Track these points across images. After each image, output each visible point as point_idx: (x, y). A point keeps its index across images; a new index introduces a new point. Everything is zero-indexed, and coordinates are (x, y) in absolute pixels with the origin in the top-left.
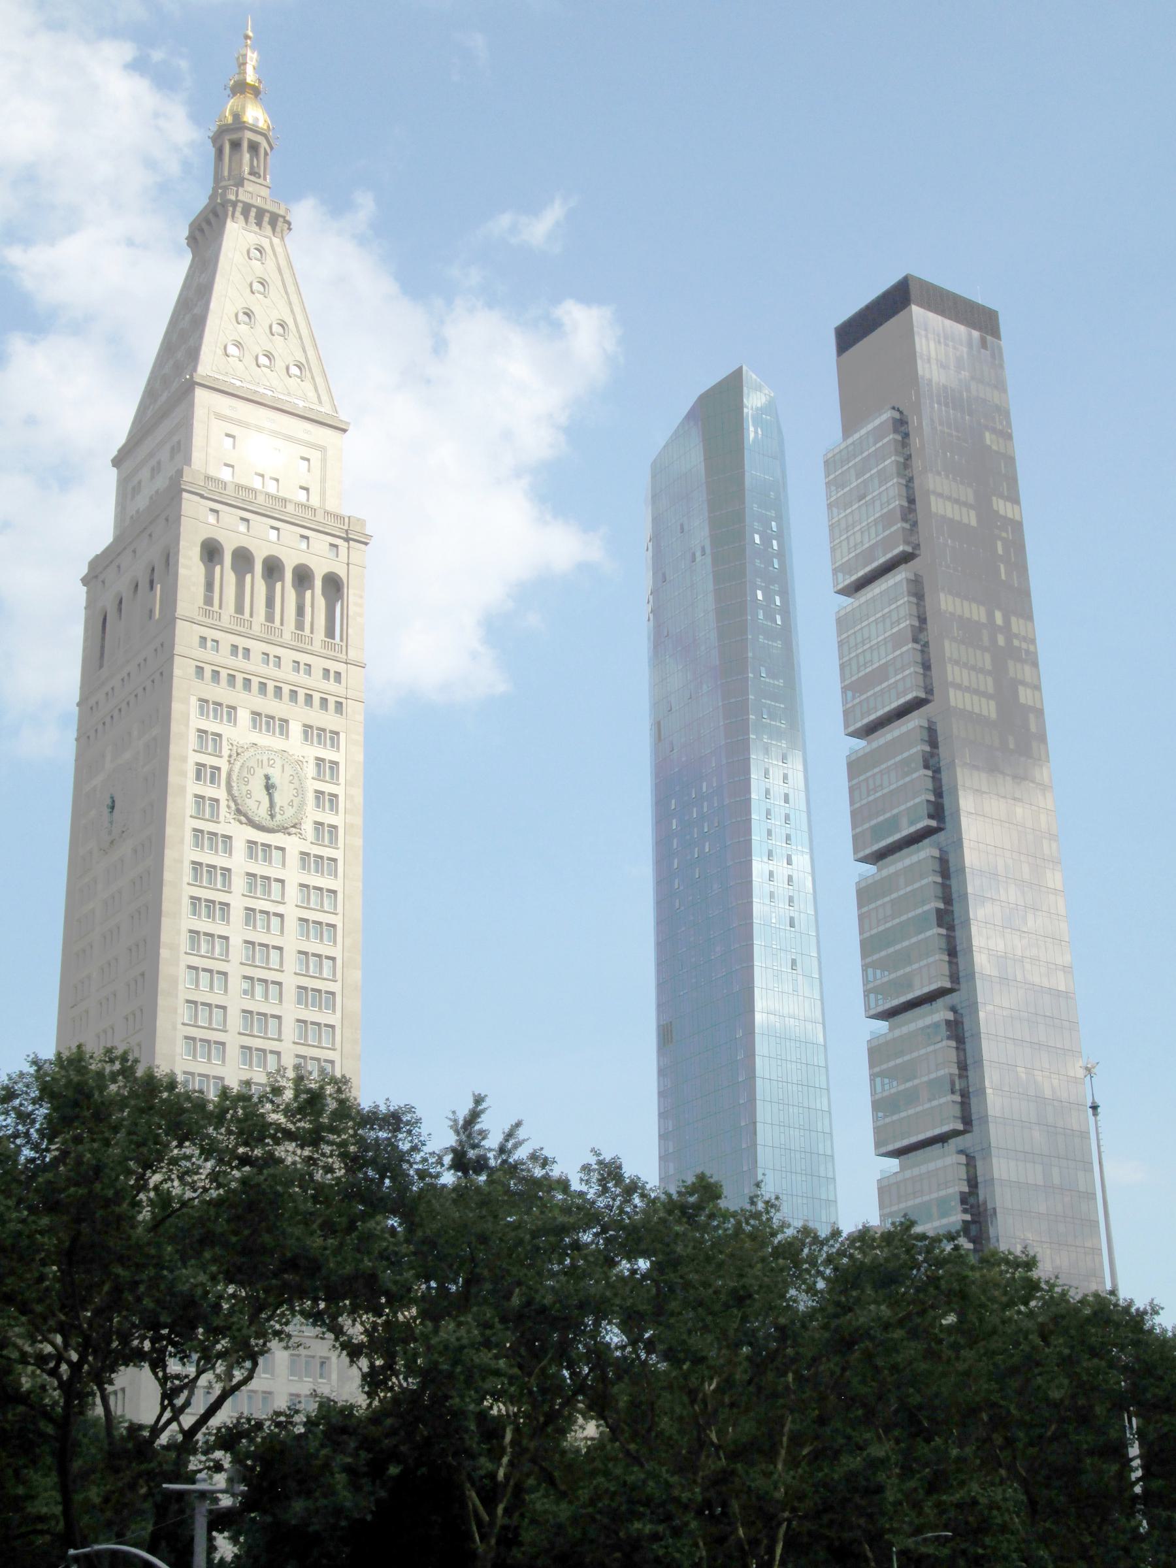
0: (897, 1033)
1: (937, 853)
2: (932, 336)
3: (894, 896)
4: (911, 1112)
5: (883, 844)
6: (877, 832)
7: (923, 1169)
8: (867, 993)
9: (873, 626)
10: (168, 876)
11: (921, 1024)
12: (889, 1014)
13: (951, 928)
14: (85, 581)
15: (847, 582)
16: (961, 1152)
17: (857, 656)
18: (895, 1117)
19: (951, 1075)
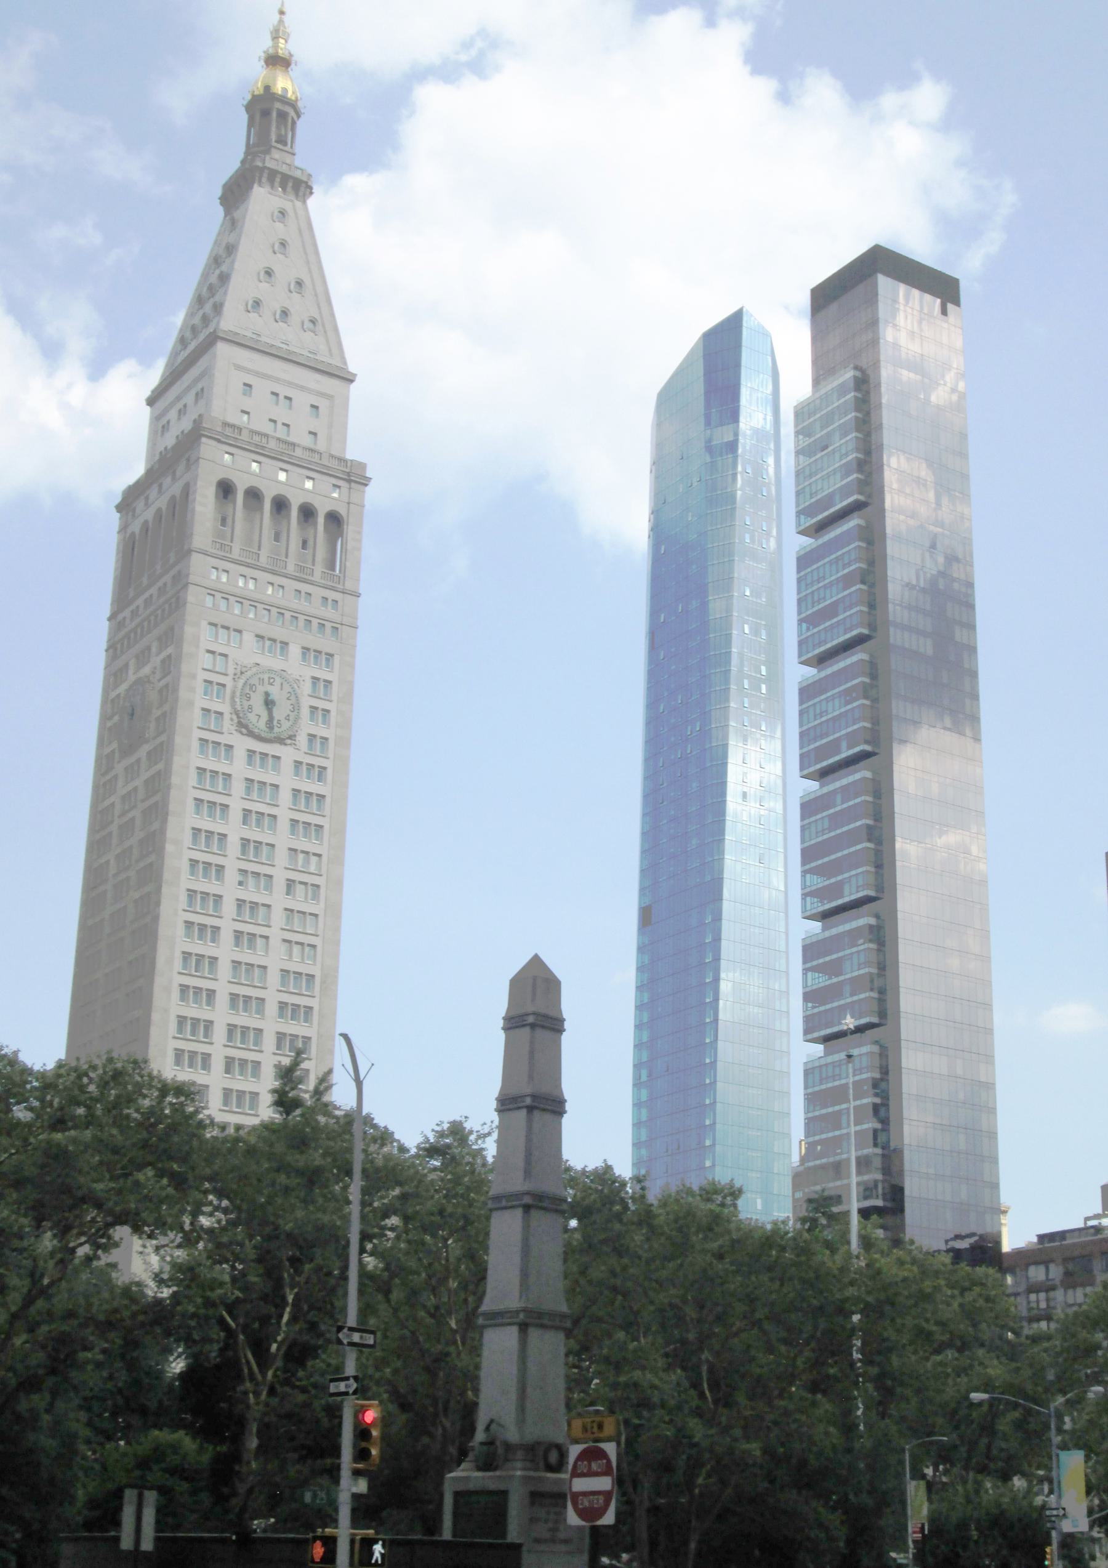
0: (827, 934)
3: (832, 811)
4: (836, 1004)
5: (825, 764)
6: (821, 753)
9: (827, 566)
10: (175, 780)
11: (847, 927)
13: (879, 842)
15: (808, 524)
16: (876, 1042)
17: (813, 592)
18: (822, 1008)
19: (871, 974)
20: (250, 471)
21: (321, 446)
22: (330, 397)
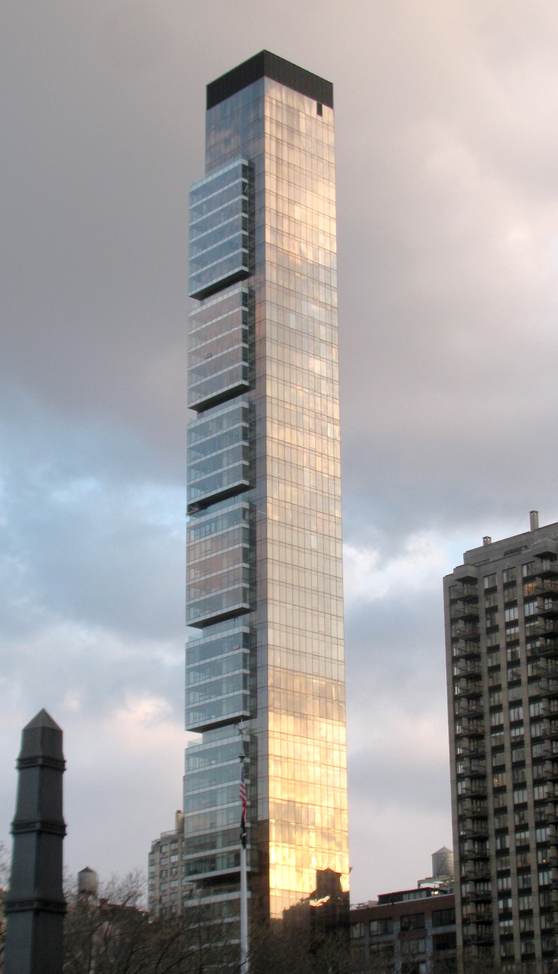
0: (208, 640)
1: (246, 506)
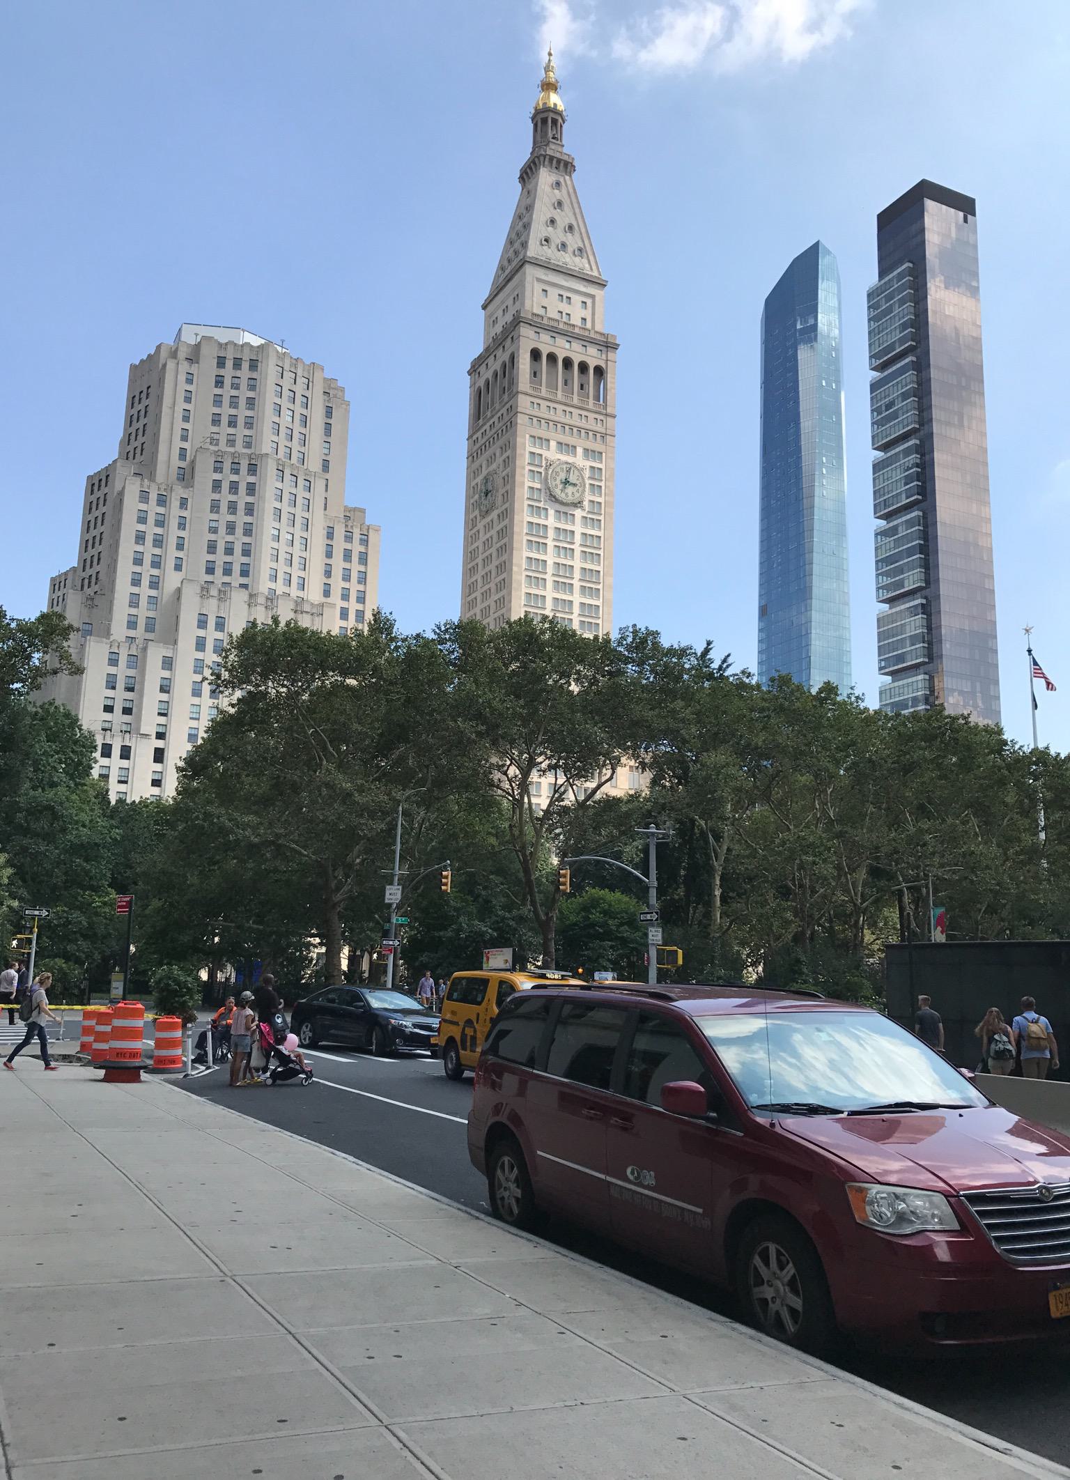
0: (894, 610)
2: (936, 216)
7: (905, 681)
8: (878, 589)
12: (891, 601)
13: (927, 555)
14: (470, 373)
20: (546, 344)
21: (589, 325)
22: (593, 297)
